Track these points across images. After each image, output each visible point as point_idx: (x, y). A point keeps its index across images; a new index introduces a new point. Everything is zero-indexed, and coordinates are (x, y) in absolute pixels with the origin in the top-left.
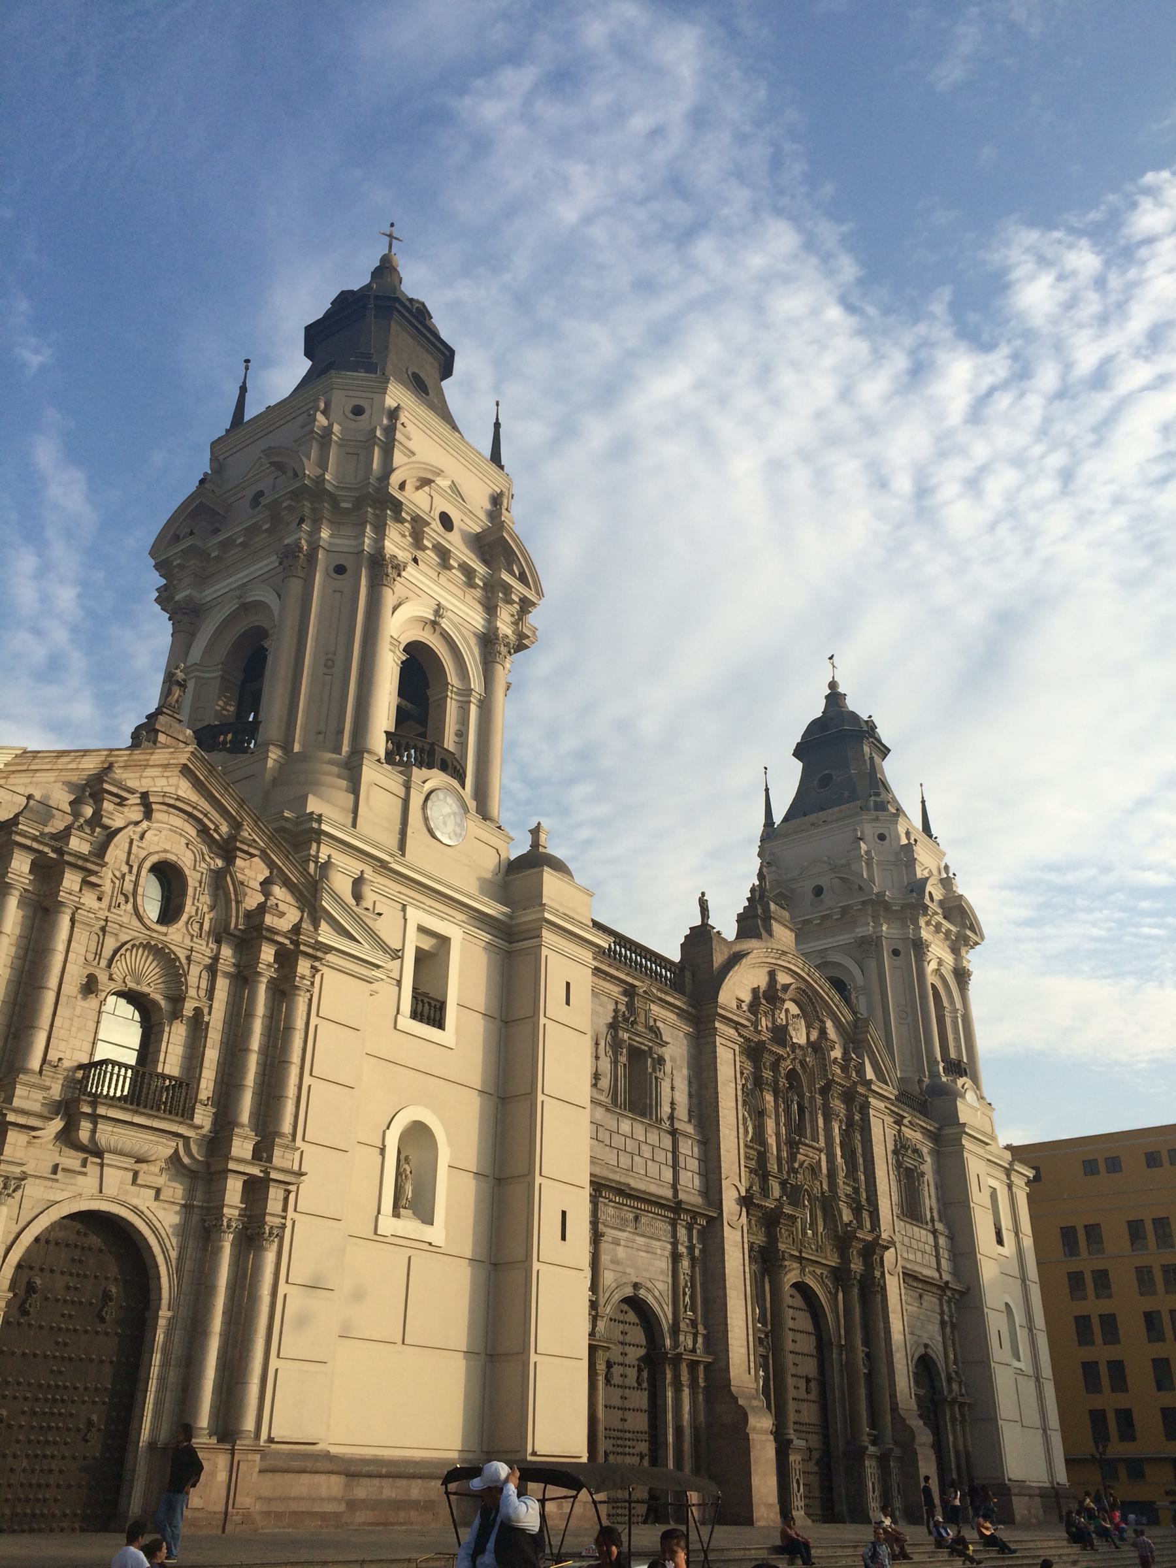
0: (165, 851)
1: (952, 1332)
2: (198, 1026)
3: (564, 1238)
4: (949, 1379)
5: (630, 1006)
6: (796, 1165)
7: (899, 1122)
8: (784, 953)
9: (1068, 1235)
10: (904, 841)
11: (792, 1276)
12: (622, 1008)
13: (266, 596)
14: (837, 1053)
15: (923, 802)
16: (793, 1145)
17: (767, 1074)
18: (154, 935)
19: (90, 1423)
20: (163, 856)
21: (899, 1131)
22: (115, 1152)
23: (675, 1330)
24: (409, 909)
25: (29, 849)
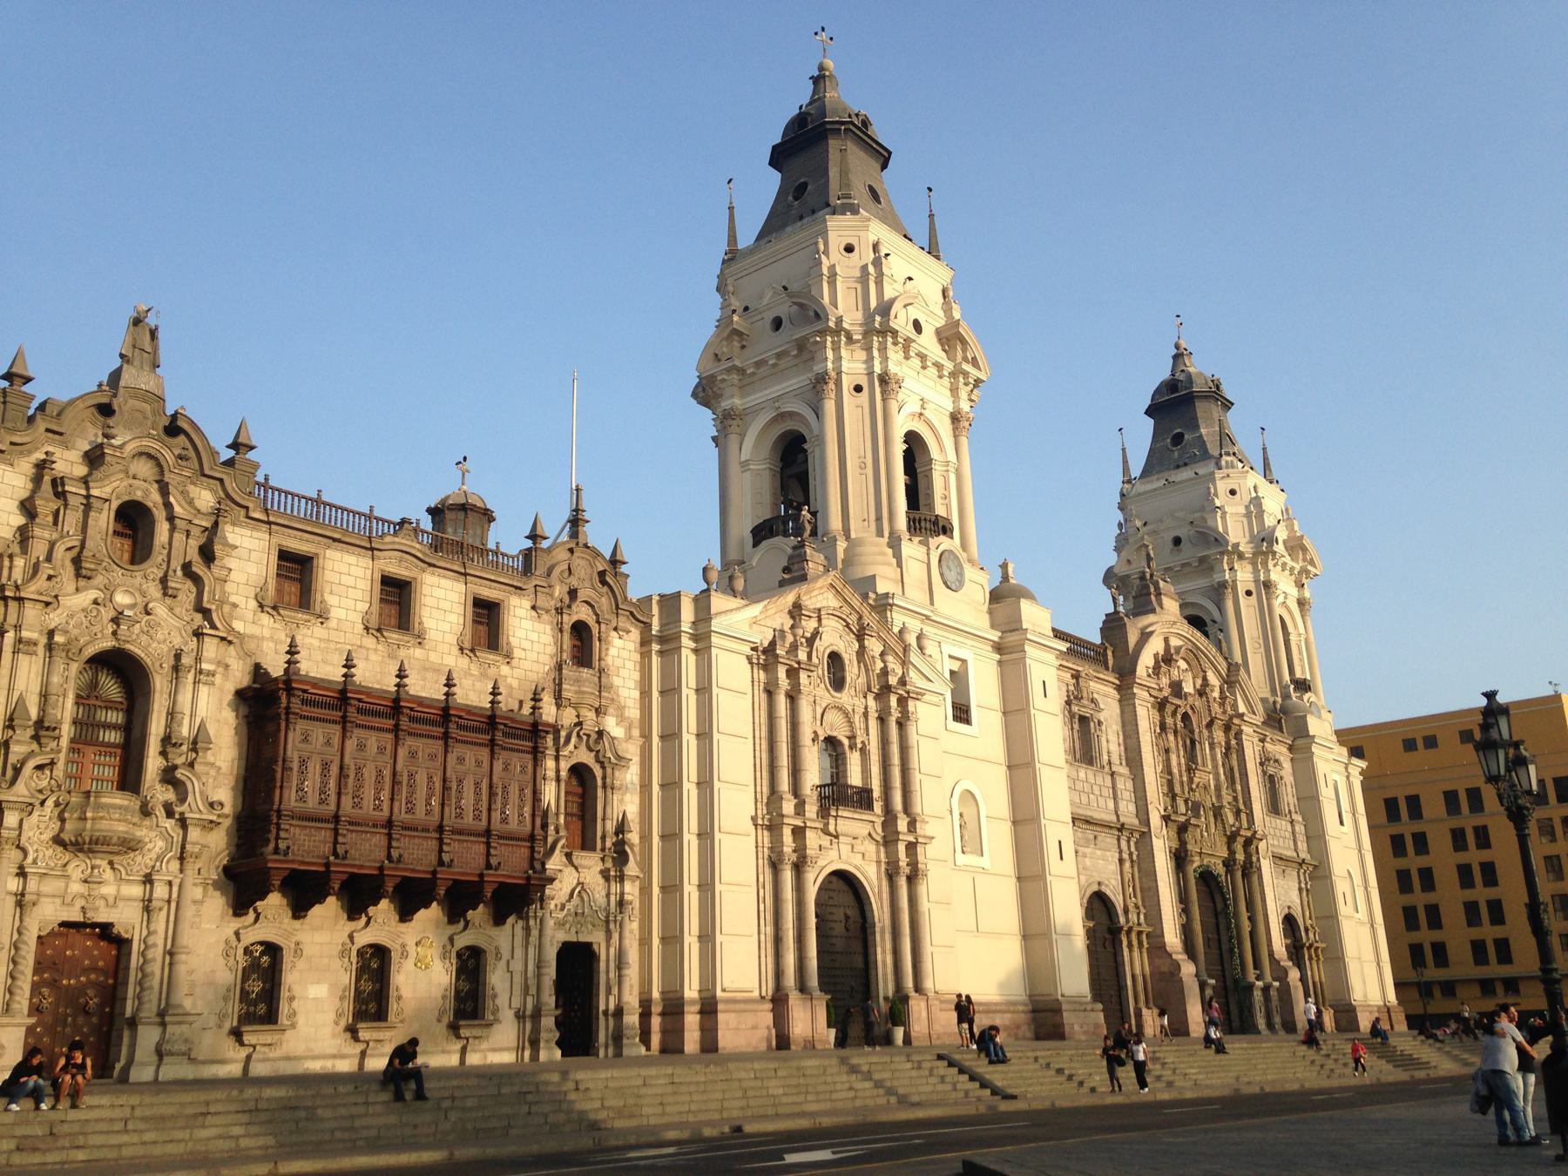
0: (832, 645)
1: (1307, 895)
2: (864, 752)
3: (1062, 858)
4: (1307, 930)
5: (1077, 685)
6: (1194, 786)
7: (1262, 741)
8: (1175, 623)
9: (1391, 806)
10: (1254, 495)
12: (1072, 688)
14: (1216, 694)
15: (1264, 449)
16: (1190, 770)
17: (1169, 721)
19: (852, 988)
23: (1126, 911)
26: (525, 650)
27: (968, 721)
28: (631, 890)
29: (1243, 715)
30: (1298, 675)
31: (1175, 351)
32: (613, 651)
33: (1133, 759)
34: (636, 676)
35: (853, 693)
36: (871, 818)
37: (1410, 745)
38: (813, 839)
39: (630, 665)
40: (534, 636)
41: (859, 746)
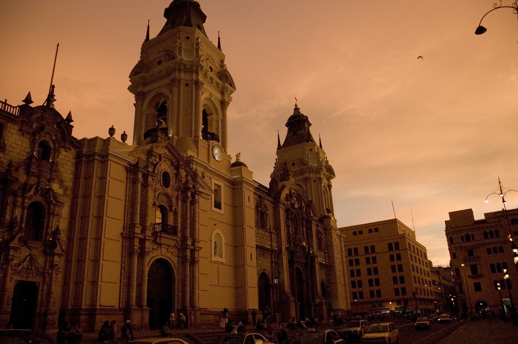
0: (165, 169)
2: (176, 213)
5: (260, 201)
6: (296, 239)
8: (293, 184)
9: (349, 251)
10: (317, 151)
11: (296, 266)
12: (258, 201)
13: (166, 91)
17: (290, 216)
18: (165, 191)
20: (165, 170)
21: (317, 228)
22: (164, 244)
24: (212, 179)
25: (142, 171)
26: (13, 148)
29: (312, 217)
30: (327, 208)
31: (295, 107)
32: (61, 156)
33: (277, 228)
34: (72, 169)
36: (176, 238)
37: (355, 233)
38: (148, 245)
39: (70, 164)
40: (20, 143)
41: (174, 210)
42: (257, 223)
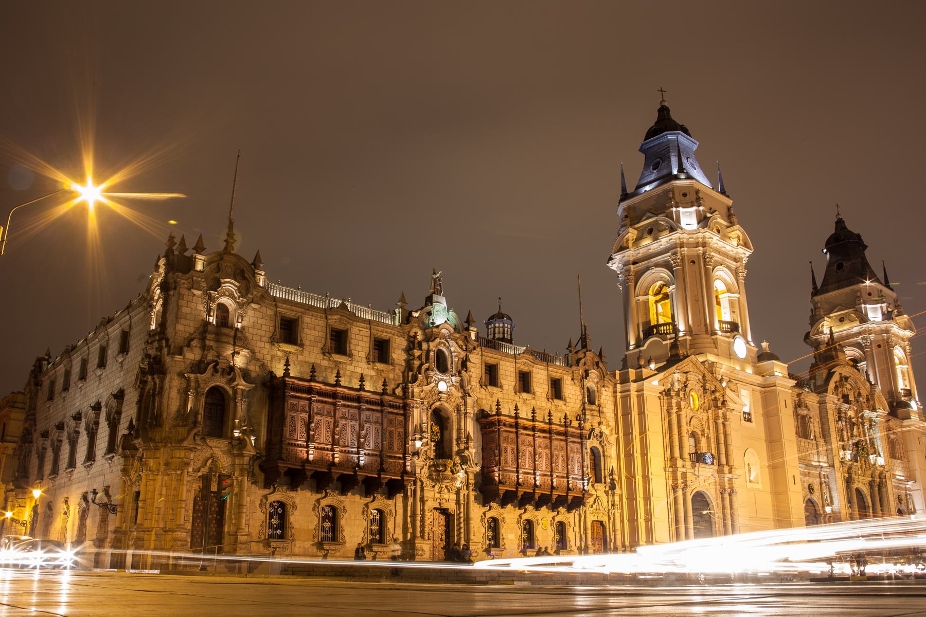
2: (708, 438)
27: (749, 420)
28: (617, 498)
34: (612, 407)
35: (702, 411)
39: (610, 402)
40: (573, 392)
41: (706, 435)
42: (797, 433)
